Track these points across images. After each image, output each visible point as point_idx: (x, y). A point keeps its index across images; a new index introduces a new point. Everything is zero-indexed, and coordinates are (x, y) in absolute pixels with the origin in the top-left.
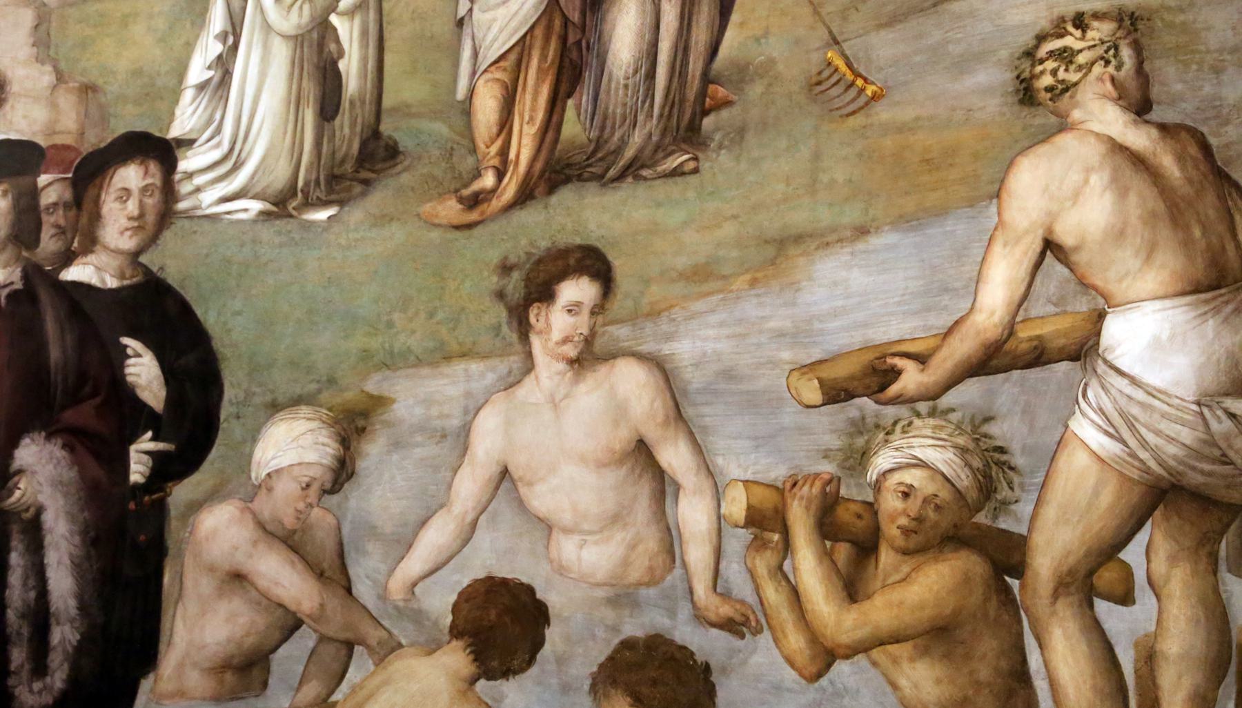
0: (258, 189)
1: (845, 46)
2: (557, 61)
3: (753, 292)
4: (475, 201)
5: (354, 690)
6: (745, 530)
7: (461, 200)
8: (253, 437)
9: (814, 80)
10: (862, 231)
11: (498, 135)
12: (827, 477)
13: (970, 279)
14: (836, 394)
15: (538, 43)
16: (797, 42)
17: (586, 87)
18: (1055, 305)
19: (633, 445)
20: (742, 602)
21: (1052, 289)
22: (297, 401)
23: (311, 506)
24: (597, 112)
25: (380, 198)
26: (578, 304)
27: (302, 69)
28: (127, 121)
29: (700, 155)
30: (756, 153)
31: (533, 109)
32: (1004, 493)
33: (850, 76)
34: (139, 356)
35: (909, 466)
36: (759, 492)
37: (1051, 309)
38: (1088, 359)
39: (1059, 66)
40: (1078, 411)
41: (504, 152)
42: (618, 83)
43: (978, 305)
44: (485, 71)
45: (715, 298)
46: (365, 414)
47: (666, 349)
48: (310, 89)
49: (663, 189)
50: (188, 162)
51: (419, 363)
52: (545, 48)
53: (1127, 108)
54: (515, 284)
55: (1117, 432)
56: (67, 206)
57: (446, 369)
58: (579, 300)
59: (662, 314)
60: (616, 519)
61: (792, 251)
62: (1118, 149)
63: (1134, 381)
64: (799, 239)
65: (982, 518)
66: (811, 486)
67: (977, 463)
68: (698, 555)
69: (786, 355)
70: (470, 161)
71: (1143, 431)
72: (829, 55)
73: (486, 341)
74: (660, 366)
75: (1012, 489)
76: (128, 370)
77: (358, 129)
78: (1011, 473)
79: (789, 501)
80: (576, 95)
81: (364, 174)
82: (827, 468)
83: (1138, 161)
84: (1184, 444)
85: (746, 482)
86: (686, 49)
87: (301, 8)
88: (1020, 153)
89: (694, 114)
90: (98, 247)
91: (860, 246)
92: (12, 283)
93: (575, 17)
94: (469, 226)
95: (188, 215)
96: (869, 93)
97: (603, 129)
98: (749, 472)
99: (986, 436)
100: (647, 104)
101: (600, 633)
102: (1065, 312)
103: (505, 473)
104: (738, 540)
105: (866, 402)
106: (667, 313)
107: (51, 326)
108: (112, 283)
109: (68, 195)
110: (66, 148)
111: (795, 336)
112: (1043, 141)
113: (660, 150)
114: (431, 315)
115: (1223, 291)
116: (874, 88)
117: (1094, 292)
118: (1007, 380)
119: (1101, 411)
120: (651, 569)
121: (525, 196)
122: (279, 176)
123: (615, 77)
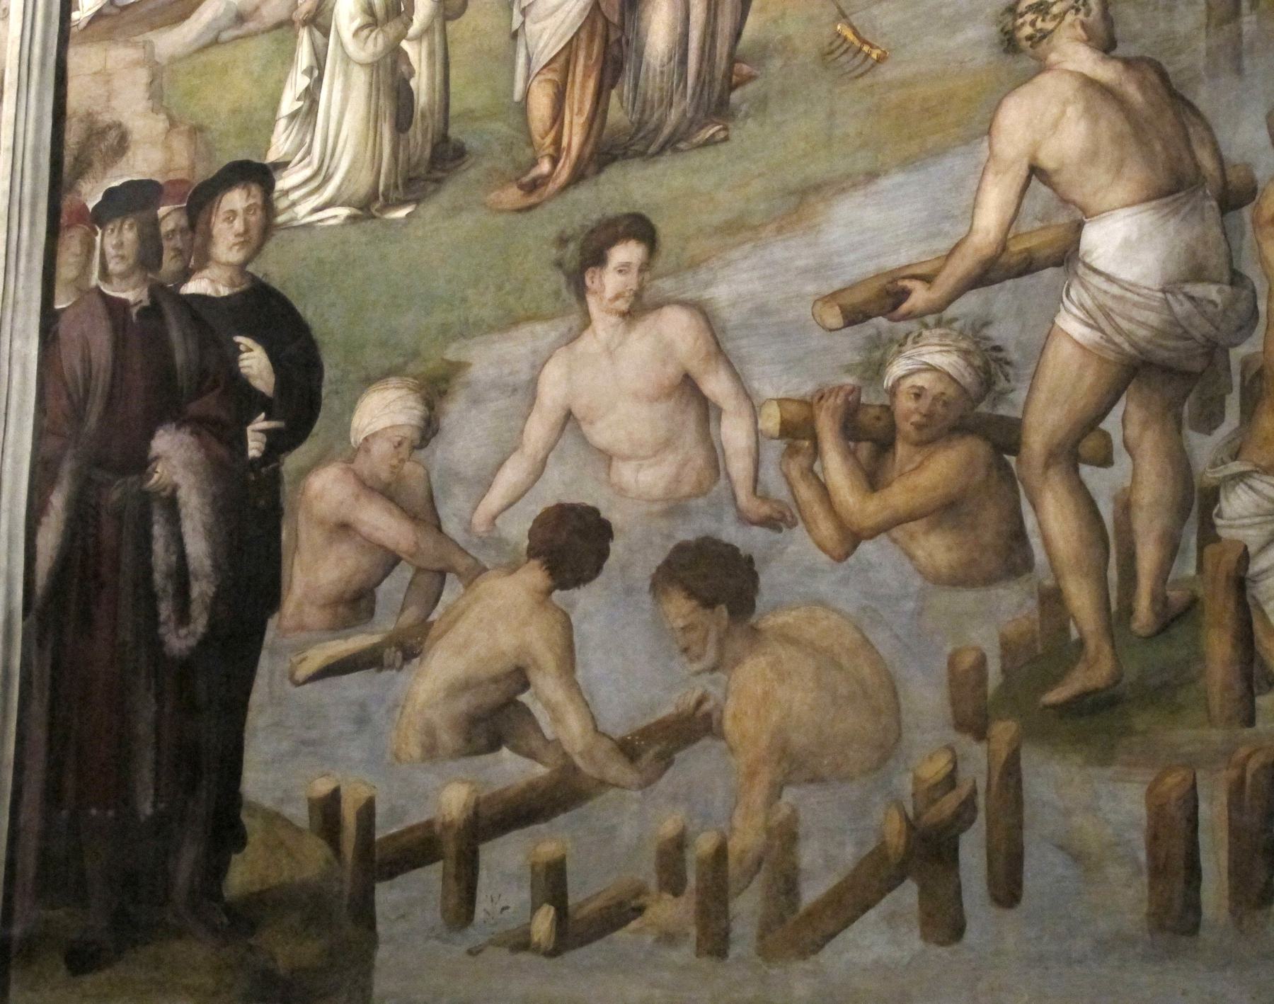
0: (345, 197)
1: (853, 18)
2: (601, 58)
3: (779, 238)
4: (533, 186)
5: (447, 611)
6: (779, 441)
7: (521, 187)
8: (351, 408)
9: (827, 50)
10: (872, 176)
11: (551, 128)
12: (849, 388)
13: (967, 206)
14: (854, 317)
15: (583, 45)
16: (811, 19)
17: (627, 79)
18: (1041, 221)
19: (679, 380)
20: (779, 502)
21: (1038, 208)
22: (386, 374)
23: (402, 461)
24: (638, 98)
25: (449, 194)
26: (627, 265)
27: (378, 90)
28: (234, 151)
29: (731, 125)
30: (777, 118)
31: (581, 102)
32: (1002, 384)
33: (857, 44)
34: (250, 350)
35: (919, 371)
36: (793, 408)
37: (1037, 224)
38: (1070, 264)
39: (1037, 18)
40: (1062, 309)
41: (557, 142)
42: (655, 70)
43: (975, 227)
44: (538, 73)
45: (748, 246)
46: (446, 379)
47: (707, 294)
48: (386, 106)
49: (696, 158)
50: (284, 182)
51: (491, 329)
55: (1096, 322)
56: (182, 231)
57: (514, 333)
58: (628, 261)
59: (702, 265)
60: (667, 444)
61: (812, 199)
62: (1089, 83)
63: (1109, 278)
65: (983, 408)
66: (836, 398)
68: (739, 467)
69: (811, 288)
70: (529, 151)
71: (1118, 320)
72: (839, 27)
73: (548, 306)
74: (703, 311)
75: (1008, 381)
76: (241, 364)
77: (429, 136)
78: (1008, 369)
79: (817, 412)
80: (618, 86)
81: (439, 174)
82: (849, 380)
84: (1152, 327)
85: (781, 402)
86: (713, 35)
87: (376, 38)
88: (1006, 95)
89: (722, 91)
90: (210, 263)
91: (873, 188)
92: (141, 301)
93: (615, 18)
94: (530, 208)
95: (286, 227)
96: (874, 56)
97: (643, 111)
98: (781, 393)
99: (987, 338)
100: (681, 86)
101: (657, 540)
103: (569, 415)
104: (774, 450)
105: (882, 322)
106: (705, 264)
107: (175, 335)
108: (224, 291)
109: (184, 222)
110: (182, 182)
111: (818, 270)
112: (1026, 82)
114: (500, 288)
115: (1182, 194)
116: (878, 52)
117: (1073, 207)
118: (1001, 289)
119: (1082, 306)
120: (700, 483)
121: (578, 177)
123: (652, 68)
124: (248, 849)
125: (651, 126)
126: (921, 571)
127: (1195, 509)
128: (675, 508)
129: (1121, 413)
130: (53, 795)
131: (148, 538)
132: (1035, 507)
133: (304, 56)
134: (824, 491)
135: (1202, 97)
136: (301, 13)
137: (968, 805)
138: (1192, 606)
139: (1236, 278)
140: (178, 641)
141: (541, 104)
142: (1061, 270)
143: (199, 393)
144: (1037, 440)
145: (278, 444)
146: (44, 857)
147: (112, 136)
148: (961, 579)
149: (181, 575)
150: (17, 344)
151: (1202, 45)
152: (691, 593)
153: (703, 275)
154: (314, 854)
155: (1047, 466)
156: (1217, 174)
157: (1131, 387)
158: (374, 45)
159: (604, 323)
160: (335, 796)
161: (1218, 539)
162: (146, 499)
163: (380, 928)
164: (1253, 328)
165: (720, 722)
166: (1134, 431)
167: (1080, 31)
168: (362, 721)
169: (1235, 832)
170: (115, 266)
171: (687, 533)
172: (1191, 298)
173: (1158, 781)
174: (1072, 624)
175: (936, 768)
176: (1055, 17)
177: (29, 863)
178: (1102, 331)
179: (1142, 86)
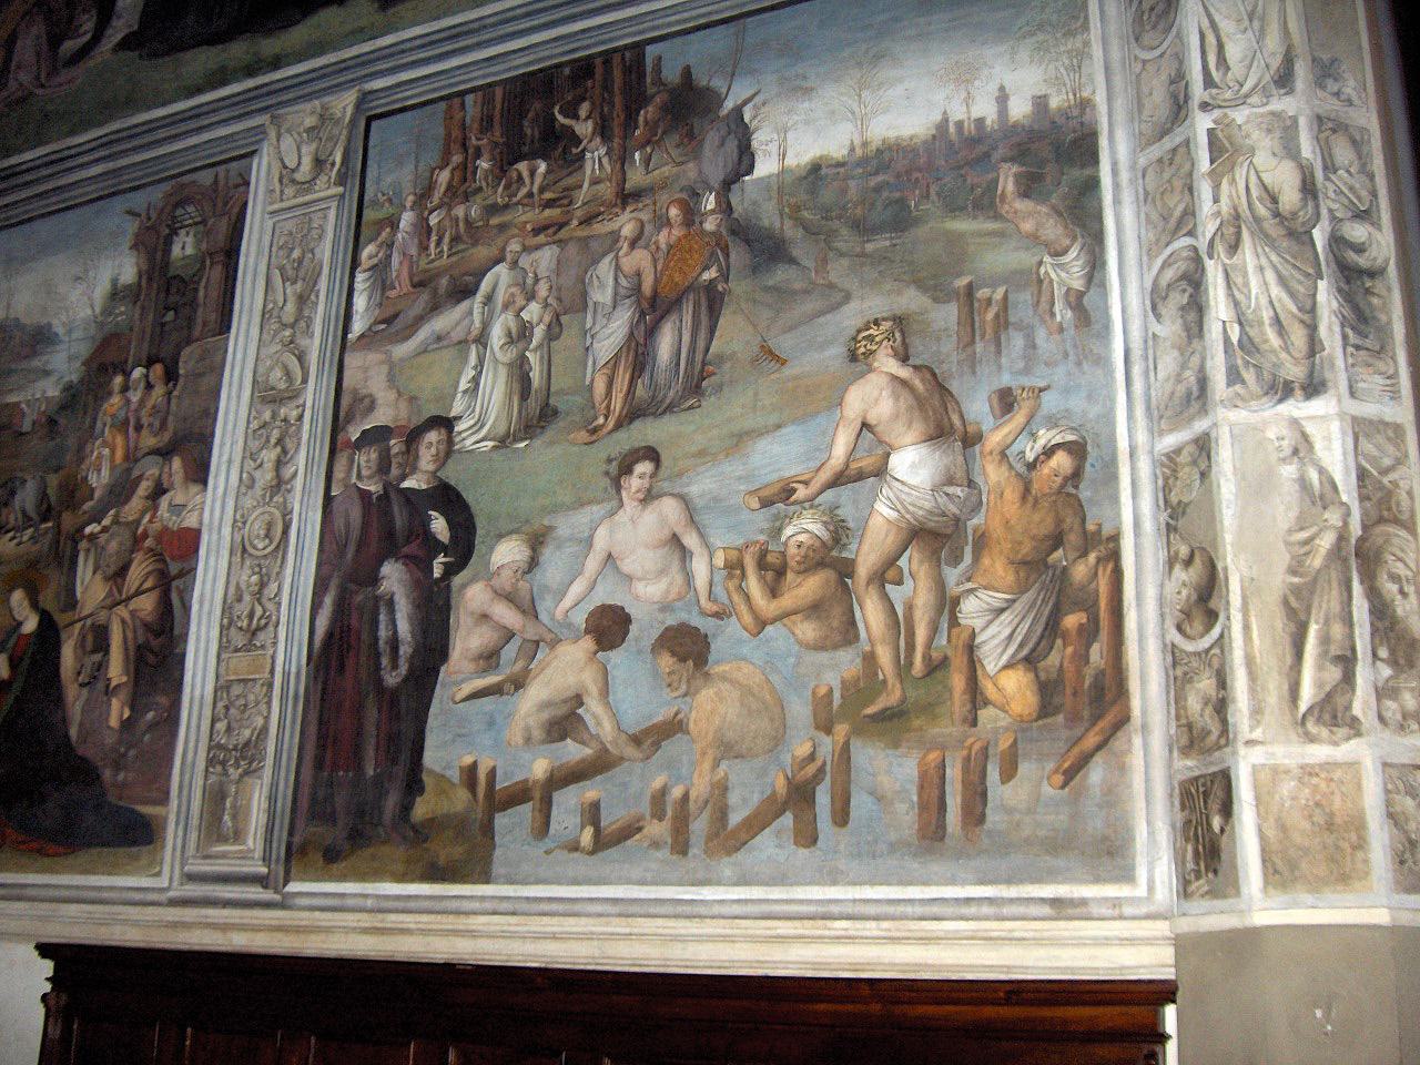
4: (594, 431)
7: (588, 431)
8: (491, 549)
10: (779, 427)
14: (766, 503)
16: (748, 343)
22: (511, 532)
25: (550, 434)
32: (845, 540)
41: (608, 407)
46: (543, 535)
47: (686, 490)
48: (516, 387)
49: (683, 416)
51: (569, 508)
52: (627, 356)
54: (614, 466)
56: (403, 453)
60: (662, 572)
62: (894, 378)
64: (747, 433)
67: (832, 528)
74: (684, 499)
81: (543, 424)
82: (762, 538)
83: (904, 383)
85: (724, 549)
91: (777, 433)
93: (642, 341)
95: (459, 451)
103: (610, 555)
104: (719, 576)
107: (396, 509)
108: (424, 487)
109: (404, 449)
113: (683, 398)
121: (619, 426)
122: (502, 430)
124: (426, 794)
125: (659, 399)
126: (800, 643)
127: (946, 611)
128: (665, 608)
130: (319, 764)
131: (375, 623)
133: (473, 359)
134: (747, 598)
135: (954, 386)
136: (471, 337)
137: (821, 770)
138: (944, 662)
139: (971, 484)
140: (391, 679)
141: (600, 387)
143: (408, 541)
144: (863, 570)
145: (450, 571)
146: (314, 800)
147: (367, 401)
148: (820, 646)
149: (394, 643)
150: (310, 513)
151: (954, 358)
152: (674, 654)
153: (685, 479)
154: (462, 795)
155: (868, 584)
158: (510, 355)
159: (630, 506)
160: (474, 765)
161: (959, 625)
162: (377, 599)
163: (496, 838)
165: (687, 724)
166: (915, 566)
168: (491, 723)
170: (365, 472)
171: (671, 621)
172: (947, 495)
173: (925, 756)
175: (803, 750)
177: (304, 802)
179: (922, 380)
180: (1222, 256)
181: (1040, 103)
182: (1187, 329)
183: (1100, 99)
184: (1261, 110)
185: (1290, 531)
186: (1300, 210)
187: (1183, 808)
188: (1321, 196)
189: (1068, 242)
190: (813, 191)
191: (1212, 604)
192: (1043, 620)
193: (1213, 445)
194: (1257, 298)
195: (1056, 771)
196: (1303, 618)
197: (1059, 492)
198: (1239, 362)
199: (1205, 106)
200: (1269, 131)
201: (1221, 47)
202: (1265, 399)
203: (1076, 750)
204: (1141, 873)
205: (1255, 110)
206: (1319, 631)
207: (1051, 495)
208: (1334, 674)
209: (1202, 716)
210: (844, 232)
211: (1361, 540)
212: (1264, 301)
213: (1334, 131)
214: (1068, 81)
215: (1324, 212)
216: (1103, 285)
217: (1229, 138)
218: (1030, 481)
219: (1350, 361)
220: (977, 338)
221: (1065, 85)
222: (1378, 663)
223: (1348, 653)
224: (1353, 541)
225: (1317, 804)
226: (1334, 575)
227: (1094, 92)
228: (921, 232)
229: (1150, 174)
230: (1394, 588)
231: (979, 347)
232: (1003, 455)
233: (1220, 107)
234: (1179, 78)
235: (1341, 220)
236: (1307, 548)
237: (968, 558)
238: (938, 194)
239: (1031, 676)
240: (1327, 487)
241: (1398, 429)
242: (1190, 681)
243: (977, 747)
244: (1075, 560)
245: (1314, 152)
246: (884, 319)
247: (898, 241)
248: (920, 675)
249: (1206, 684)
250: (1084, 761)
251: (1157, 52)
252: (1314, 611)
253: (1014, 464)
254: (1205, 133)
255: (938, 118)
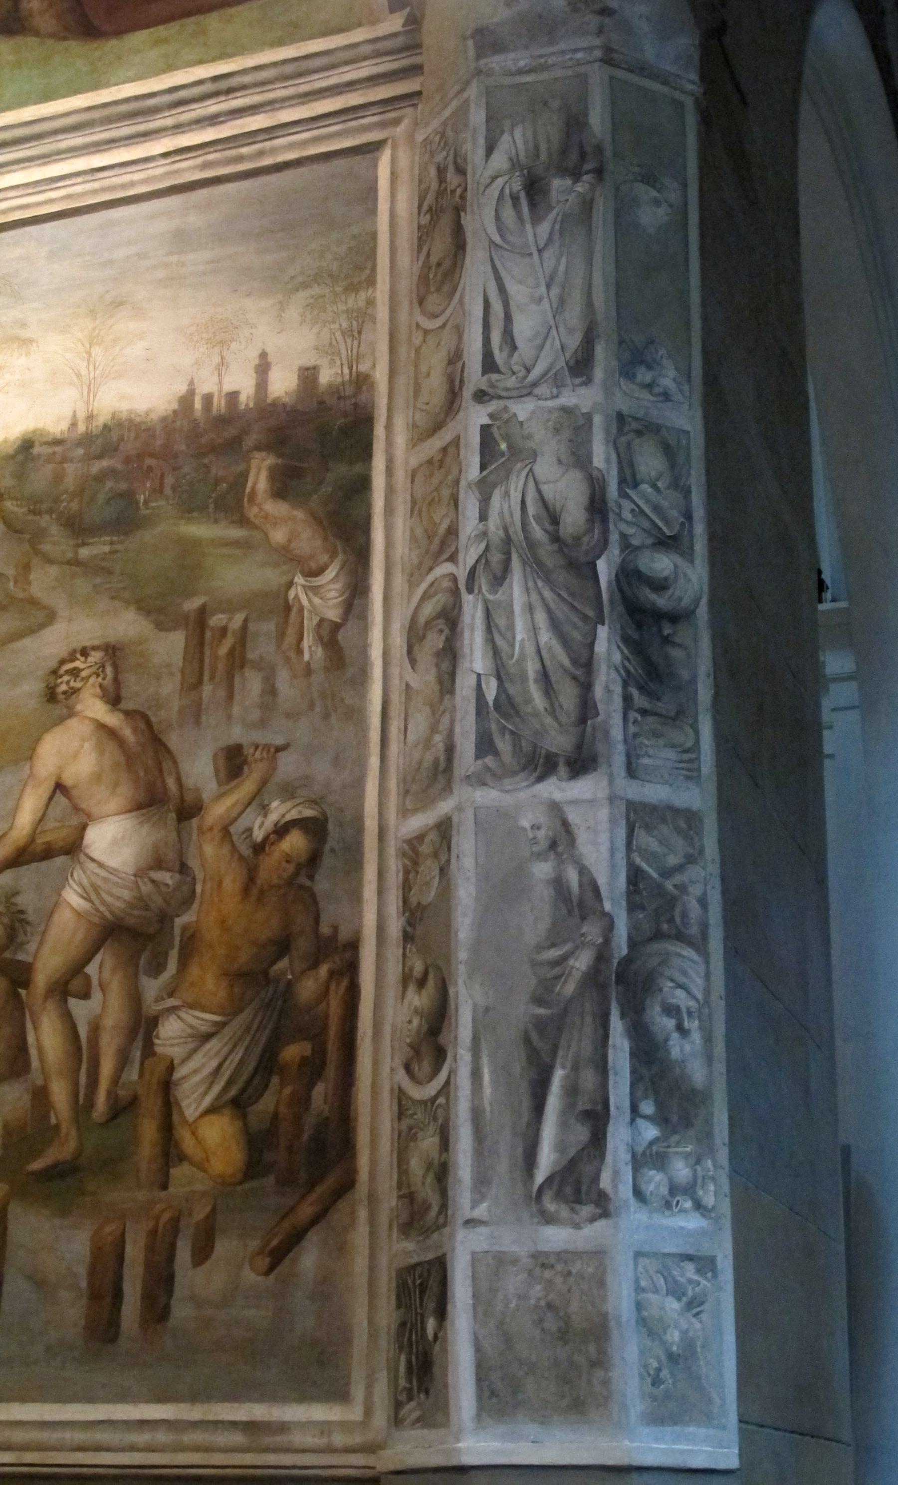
32: (21, 938)
37: (57, 824)
53: (107, 702)
62: (101, 727)
63: (100, 865)
65: (7, 955)
71: (104, 895)
75: (26, 935)
83: (111, 733)
99: (15, 904)
102: (63, 826)
119: (80, 884)
127: (142, 1031)
129: (99, 961)
132: (36, 1028)
135: (173, 740)
138: (134, 1101)
139: (183, 869)
142: (70, 856)
144: (41, 978)
151: (176, 705)
155: (46, 997)
156: (177, 794)
157: (107, 943)
161: (154, 1054)
164: (192, 904)
166: (106, 974)
167: (98, 690)
169: (149, 1266)
172: (153, 881)
174: (52, 1112)
176: (83, 679)
178: (90, 901)
179: (135, 730)
180: (484, 589)
181: (308, 375)
182: (440, 682)
183: (381, 376)
184: (550, 404)
185: (539, 948)
186: (585, 534)
187: (399, 1306)
188: (612, 517)
189: (325, 558)
190: (21, 476)
191: (442, 1039)
192: (258, 1050)
193: (454, 832)
194: (522, 647)
195: (260, 1252)
196: (547, 1060)
197: (290, 882)
198: (494, 727)
199: (481, 396)
200: (557, 430)
201: (508, 318)
202: (522, 775)
203: (286, 1225)
204: (358, 1392)
205: (541, 403)
206: (567, 1077)
207: (280, 887)
208: (581, 1134)
209: (423, 1184)
210: (54, 530)
211: (627, 961)
212: (530, 650)
213: (639, 433)
214: (344, 352)
215: (614, 537)
216: (364, 616)
217: (507, 438)
218: (257, 866)
219: (632, 729)
220: (206, 678)
221: (339, 354)
222: (640, 1122)
223: (599, 1108)
224: (615, 962)
225: (550, 1306)
226: (588, 1006)
227: (374, 366)
228: (148, 536)
229: (419, 479)
230: (670, 1023)
231: (207, 689)
232: (226, 832)
233: (500, 397)
234: (455, 358)
235: (637, 548)
236: (557, 971)
237: (172, 966)
238: (174, 489)
239: (238, 1124)
240: (589, 895)
241: (691, 817)
242: (414, 1138)
243: (166, 1216)
244: (303, 972)
245: (608, 461)
246: (94, 648)
247: (118, 547)
248: (102, 1120)
249: (429, 1143)
250: (296, 1237)
251: (439, 322)
252: (561, 1053)
253: (237, 844)
254: (478, 429)
255: (182, 389)
